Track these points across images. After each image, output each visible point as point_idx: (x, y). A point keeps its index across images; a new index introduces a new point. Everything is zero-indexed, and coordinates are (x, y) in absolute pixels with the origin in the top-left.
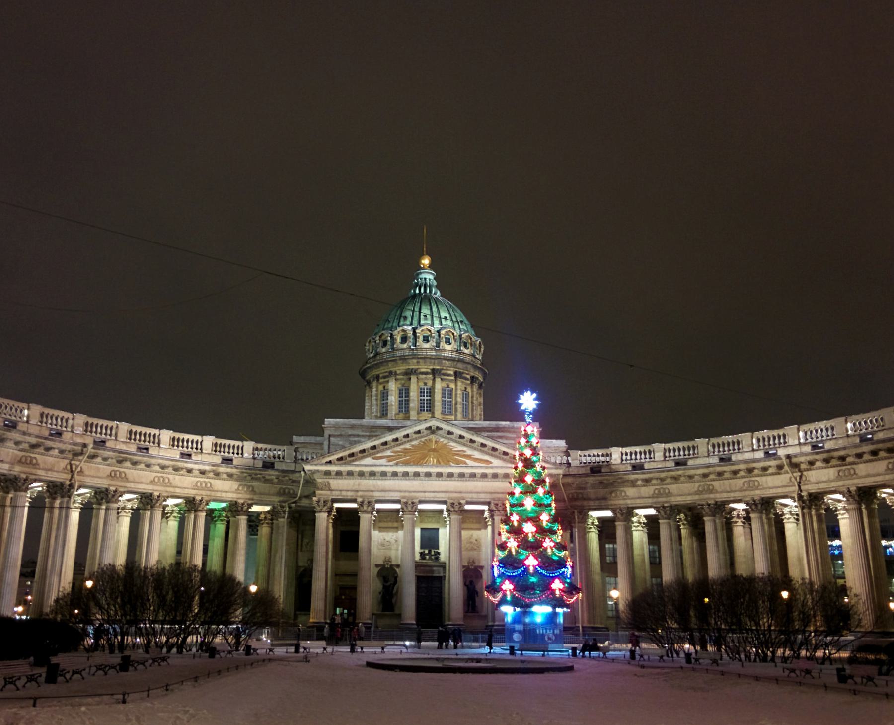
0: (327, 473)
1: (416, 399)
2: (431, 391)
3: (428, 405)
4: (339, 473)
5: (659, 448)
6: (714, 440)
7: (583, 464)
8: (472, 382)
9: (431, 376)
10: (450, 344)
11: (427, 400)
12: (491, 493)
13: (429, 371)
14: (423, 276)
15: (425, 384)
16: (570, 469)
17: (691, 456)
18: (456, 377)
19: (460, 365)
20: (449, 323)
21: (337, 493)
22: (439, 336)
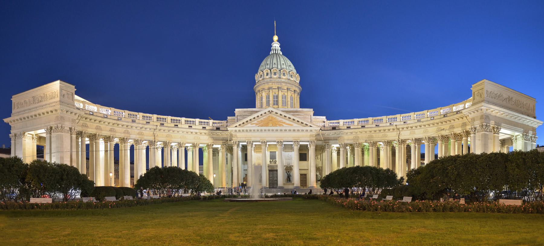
0: (236, 131)
1: (272, 100)
2: (277, 97)
3: (277, 102)
4: (239, 131)
5: (356, 120)
6: (375, 118)
7: (329, 126)
8: (294, 93)
9: (277, 90)
10: (285, 76)
11: (276, 100)
12: (293, 137)
13: (276, 88)
14: (274, 45)
15: (275, 93)
16: (325, 128)
17: (367, 124)
18: (287, 90)
19: (289, 85)
20: (285, 66)
21: (240, 139)
22: (280, 72)
